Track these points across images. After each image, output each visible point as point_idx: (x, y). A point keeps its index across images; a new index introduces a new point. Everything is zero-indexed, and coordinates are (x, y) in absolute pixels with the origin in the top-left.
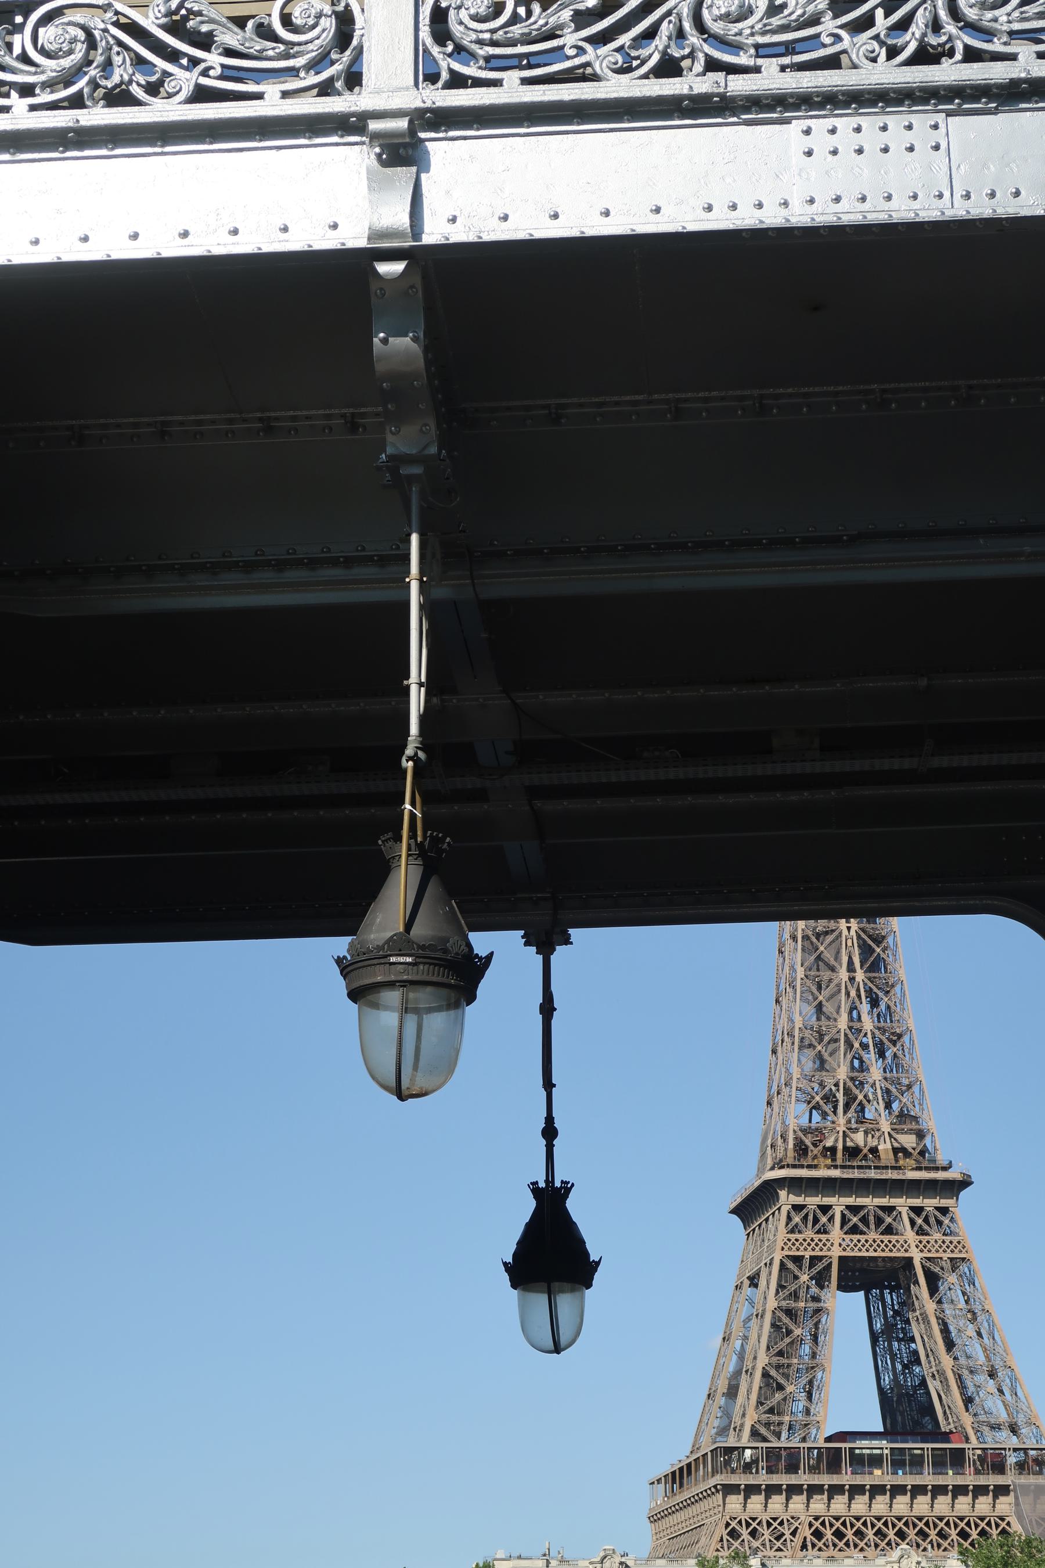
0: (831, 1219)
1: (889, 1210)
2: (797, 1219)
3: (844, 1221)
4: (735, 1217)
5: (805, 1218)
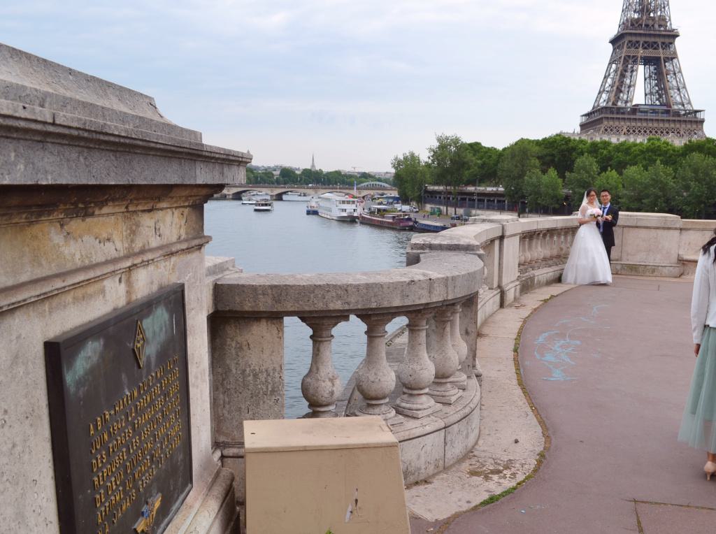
0: (639, 46)
1: (655, 43)
2: (629, 45)
3: (643, 45)
4: (610, 45)
5: (632, 45)
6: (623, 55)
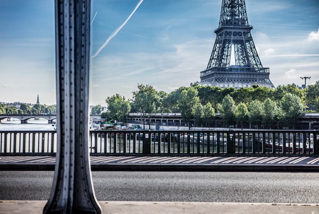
0: (231, 34)
1: (240, 32)
3: (233, 34)
5: (227, 34)
6: (223, 39)
